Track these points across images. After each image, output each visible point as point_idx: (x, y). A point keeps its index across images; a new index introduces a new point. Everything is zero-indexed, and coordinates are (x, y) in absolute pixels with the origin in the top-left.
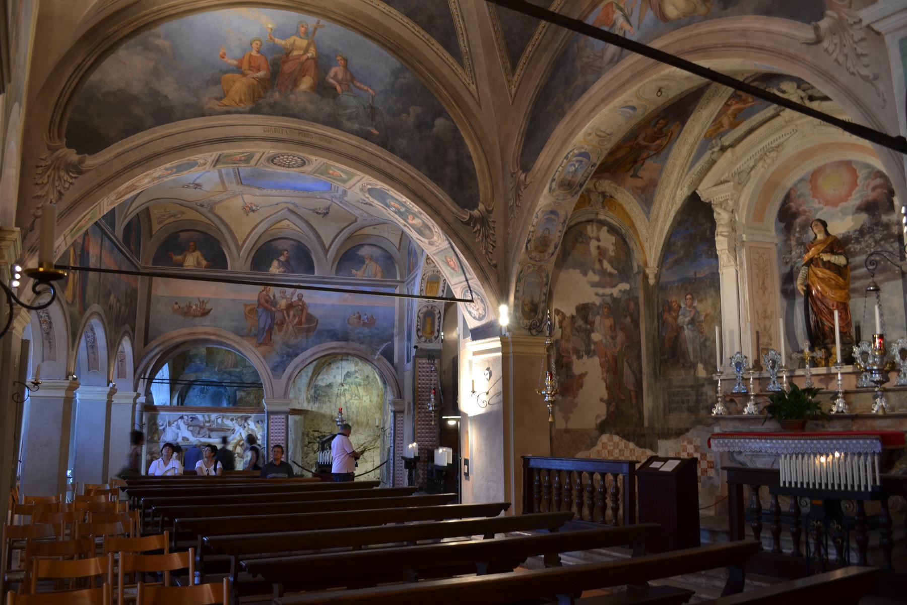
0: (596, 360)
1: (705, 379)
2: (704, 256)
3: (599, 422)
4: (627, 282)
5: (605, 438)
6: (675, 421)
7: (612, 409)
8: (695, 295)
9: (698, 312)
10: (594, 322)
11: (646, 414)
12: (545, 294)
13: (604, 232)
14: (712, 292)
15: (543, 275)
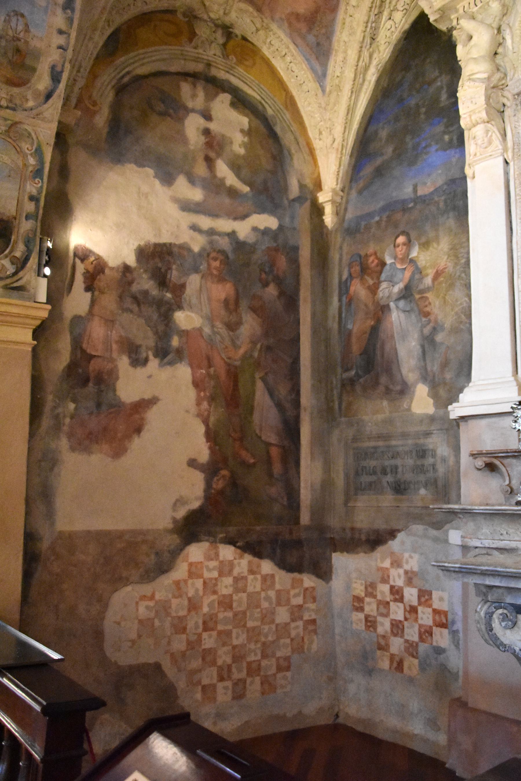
0: (184, 372)
1: (432, 419)
2: (433, 148)
3: (181, 513)
4: (272, 213)
5: (196, 552)
6: (366, 513)
7: (219, 484)
8: (413, 234)
9: (419, 271)
10: (183, 286)
11: (306, 496)
12: (32, 198)
13: (221, 106)
14: (451, 222)
15: (25, 146)
